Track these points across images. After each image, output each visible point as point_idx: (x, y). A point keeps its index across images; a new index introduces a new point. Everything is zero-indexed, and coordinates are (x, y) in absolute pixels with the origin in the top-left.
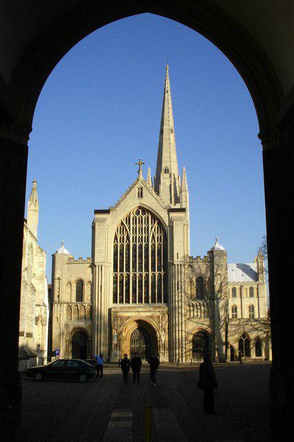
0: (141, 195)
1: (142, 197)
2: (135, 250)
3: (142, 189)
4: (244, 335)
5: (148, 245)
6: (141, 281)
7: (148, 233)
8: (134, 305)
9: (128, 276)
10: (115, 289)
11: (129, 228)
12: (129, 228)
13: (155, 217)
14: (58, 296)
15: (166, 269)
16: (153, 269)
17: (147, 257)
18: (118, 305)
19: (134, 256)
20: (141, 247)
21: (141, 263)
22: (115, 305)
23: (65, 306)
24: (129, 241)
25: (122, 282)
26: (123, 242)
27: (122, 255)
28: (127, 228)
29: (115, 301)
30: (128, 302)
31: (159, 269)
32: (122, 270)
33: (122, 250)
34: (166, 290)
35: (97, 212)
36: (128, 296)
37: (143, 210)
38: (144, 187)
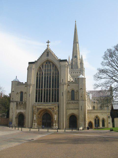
0: (48, 55)
1: (48, 56)
3: (48, 52)
4: (97, 117)
5: (50, 77)
9: (42, 90)
10: (36, 96)
12: (43, 69)
13: (54, 65)
14: (13, 99)
15: (58, 87)
16: (53, 87)
17: (50, 82)
19: (45, 82)
21: (47, 85)
23: (16, 103)
25: (39, 93)
27: (40, 81)
29: (36, 101)
31: (55, 87)
32: (39, 88)
33: (40, 79)
34: (58, 96)
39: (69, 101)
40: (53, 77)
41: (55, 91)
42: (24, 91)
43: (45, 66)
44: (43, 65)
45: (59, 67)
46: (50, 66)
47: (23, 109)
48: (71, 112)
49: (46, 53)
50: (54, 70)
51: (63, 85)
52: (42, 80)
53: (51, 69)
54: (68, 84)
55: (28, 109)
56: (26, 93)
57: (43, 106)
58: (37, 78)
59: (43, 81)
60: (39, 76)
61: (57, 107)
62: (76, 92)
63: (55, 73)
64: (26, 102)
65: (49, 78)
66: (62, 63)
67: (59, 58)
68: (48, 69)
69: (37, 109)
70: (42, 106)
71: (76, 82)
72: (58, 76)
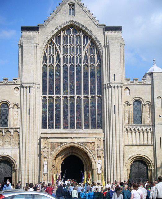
2: (65, 72)
3: (73, 5)
5: (79, 66)
6: (72, 105)
7: (80, 53)
8: (66, 131)
10: (44, 113)
11: (59, 47)
12: (59, 47)
13: (87, 36)
15: (100, 92)
16: (86, 92)
17: (79, 79)
18: (48, 130)
19: (65, 78)
20: (72, 69)
22: (44, 131)
24: (60, 62)
25: (51, 106)
26: (53, 62)
27: (51, 76)
28: (58, 47)
30: (58, 127)
31: (93, 92)
32: (51, 93)
33: (51, 71)
35: (25, 29)
36: (58, 121)
37: (73, 27)
38: (76, 3)
39: (130, 127)
40: (86, 66)
41: (93, 103)
42: (11, 102)
43: (65, 37)
44: (60, 37)
45: (103, 44)
46: (77, 39)
47: (10, 147)
48: (135, 154)
49: (66, 7)
50: (87, 50)
51: (114, 87)
52: (56, 74)
53: (80, 47)
54: (126, 86)
55: (27, 147)
56: (17, 106)
57: (66, 138)
58: (44, 67)
59: (60, 76)
60: (50, 62)
61: (102, 140)
62: (145, 105)
63: (91, 58)
64: (18, 128)
65: (76, 68)
66: (109, 34)
67: (100, 23)
68: (73, 47)
69: (51, 146)
70: (63, 138)
71: (144, 81)
72: (100, 66)
